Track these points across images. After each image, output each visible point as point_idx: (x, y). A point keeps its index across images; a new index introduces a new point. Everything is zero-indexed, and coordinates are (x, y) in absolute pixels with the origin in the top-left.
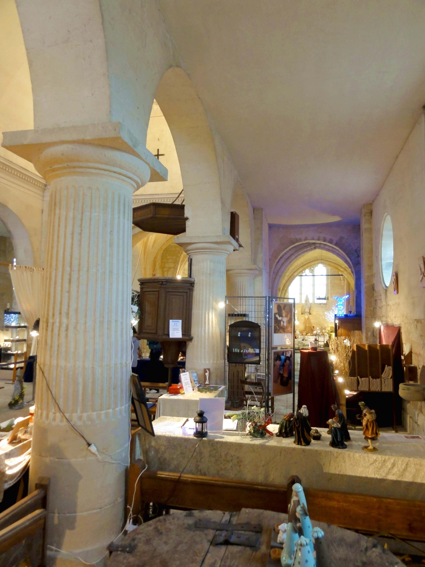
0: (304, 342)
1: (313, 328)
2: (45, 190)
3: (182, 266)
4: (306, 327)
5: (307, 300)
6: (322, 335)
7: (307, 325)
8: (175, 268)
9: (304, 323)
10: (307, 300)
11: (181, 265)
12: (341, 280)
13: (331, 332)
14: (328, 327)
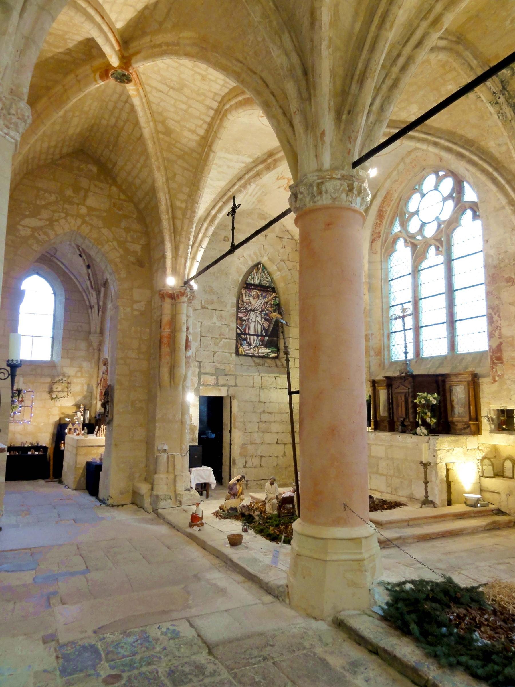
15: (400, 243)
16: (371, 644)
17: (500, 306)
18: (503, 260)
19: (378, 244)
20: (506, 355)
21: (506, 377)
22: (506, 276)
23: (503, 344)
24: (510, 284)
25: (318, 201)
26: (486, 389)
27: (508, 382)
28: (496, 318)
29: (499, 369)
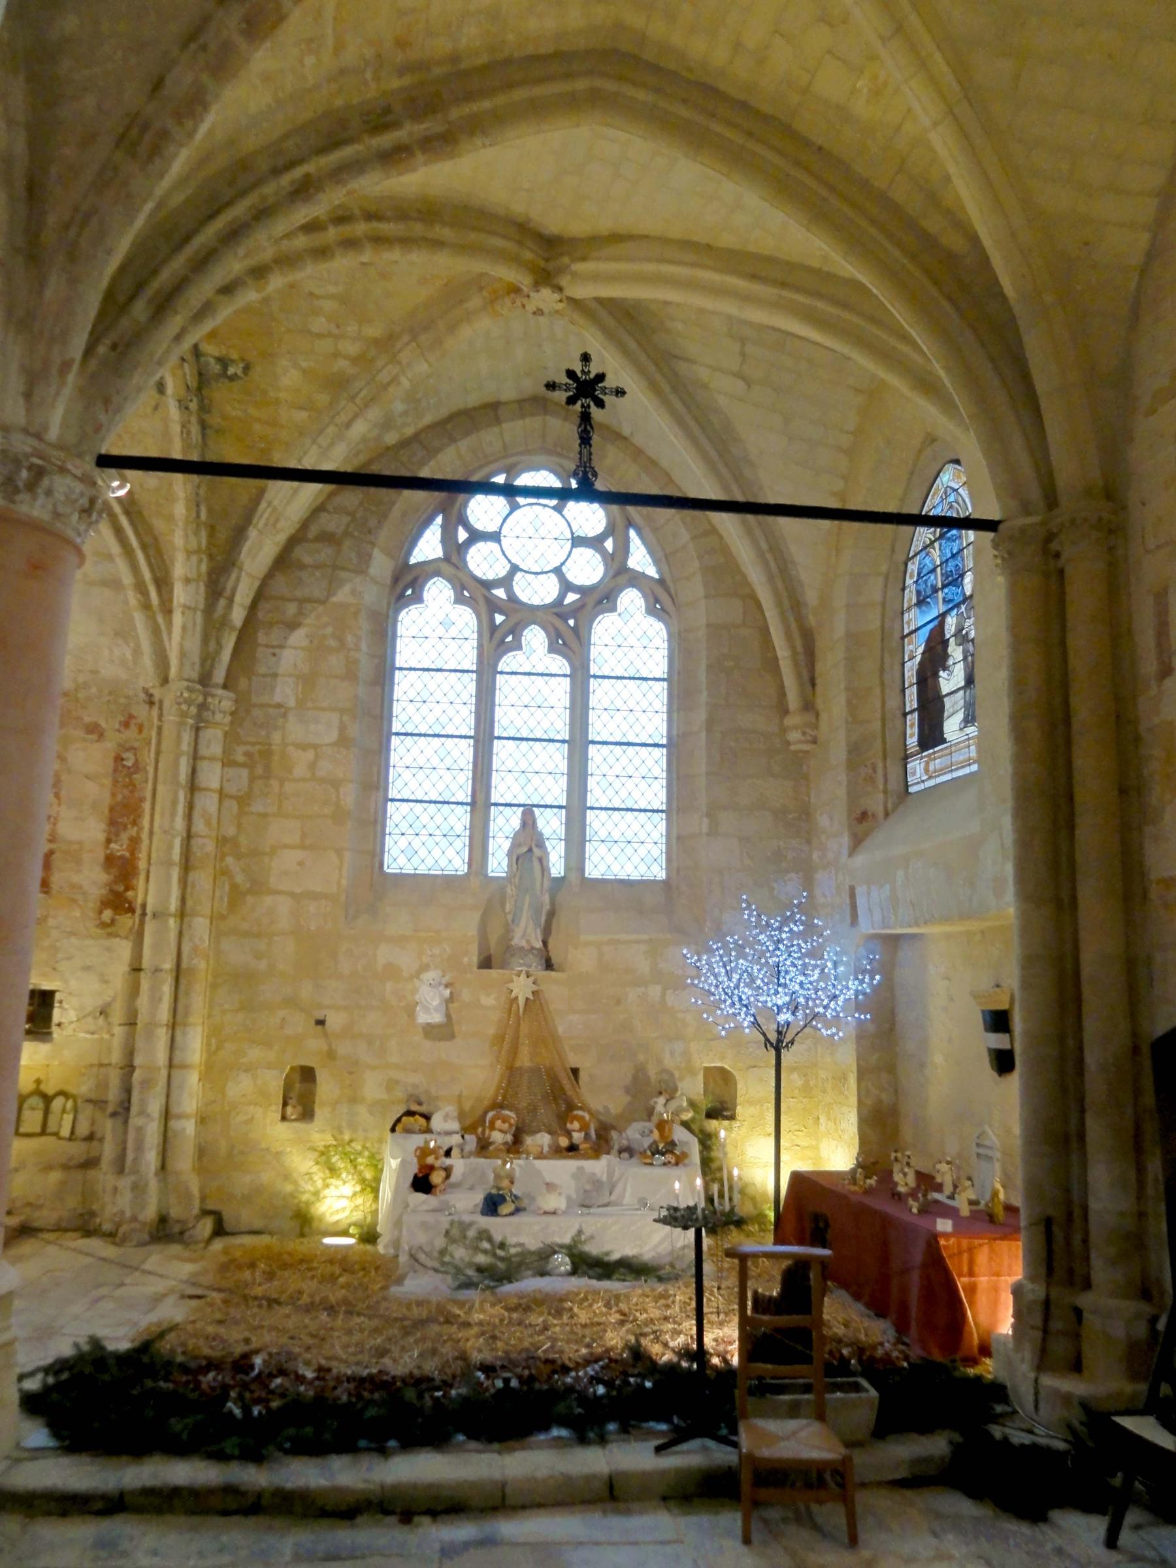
0: (499, 1227)
1: (566, 1083)
4: (512, 1072)
5: (528, 847)
6: (656, 1151)
7: (525, 1060)
9: (499, 1039)
10: (528, 847)
12: (785, 711)
13: (712, 1114)
14: (692, 1072)
16: (104, 1497)
17: (64, 777)
18: (86, 686)
21: (51, 922)
22: (87, 719)
24: (94, 737)
25: (21, 502)
27: (55, 934)
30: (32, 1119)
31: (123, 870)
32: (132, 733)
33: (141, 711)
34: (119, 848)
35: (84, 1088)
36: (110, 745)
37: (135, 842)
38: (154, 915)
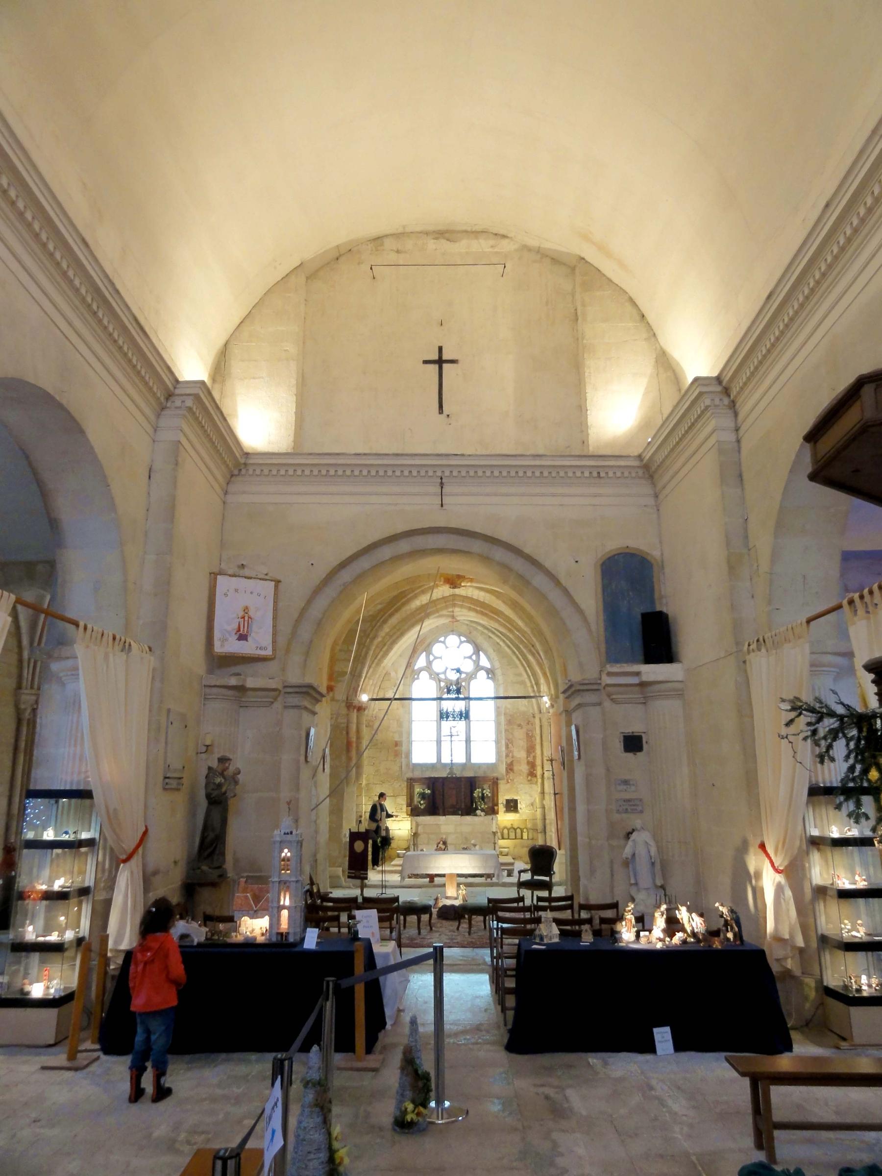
2: (163, 409)
3: (371, 670)
8: (356, 676)
11: (370, 667)
15: (424, 675)
19: (409, 671)
20: (515, 768)
23: (514, 764)
26: (502, 786)
28: (510, 745)
29: (511, 775)
30: (512, 835)
31: (532, 765)
32: (530, 726)
33: (532, 719)
34: (531, 759)
35: (529, 826)
36: (524, 730)
37: (535, 757)
38: (548, 778)
